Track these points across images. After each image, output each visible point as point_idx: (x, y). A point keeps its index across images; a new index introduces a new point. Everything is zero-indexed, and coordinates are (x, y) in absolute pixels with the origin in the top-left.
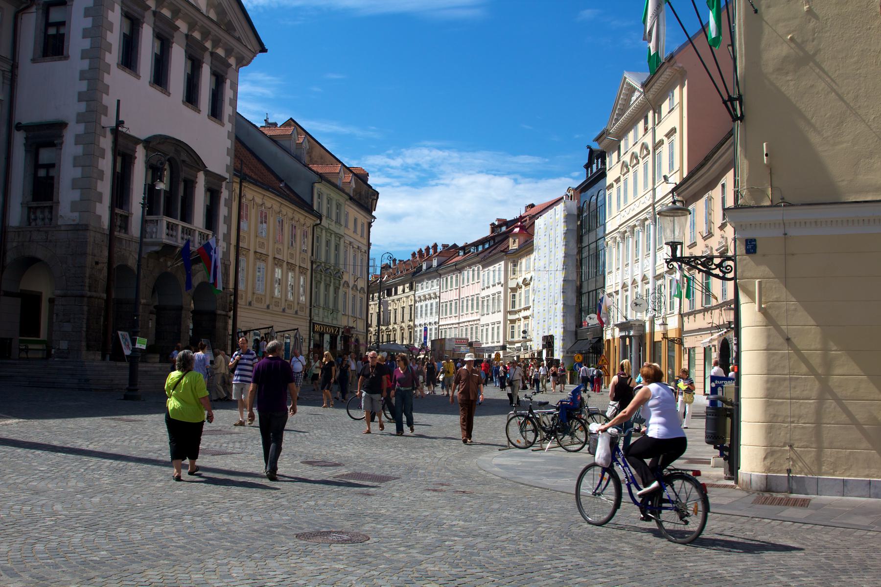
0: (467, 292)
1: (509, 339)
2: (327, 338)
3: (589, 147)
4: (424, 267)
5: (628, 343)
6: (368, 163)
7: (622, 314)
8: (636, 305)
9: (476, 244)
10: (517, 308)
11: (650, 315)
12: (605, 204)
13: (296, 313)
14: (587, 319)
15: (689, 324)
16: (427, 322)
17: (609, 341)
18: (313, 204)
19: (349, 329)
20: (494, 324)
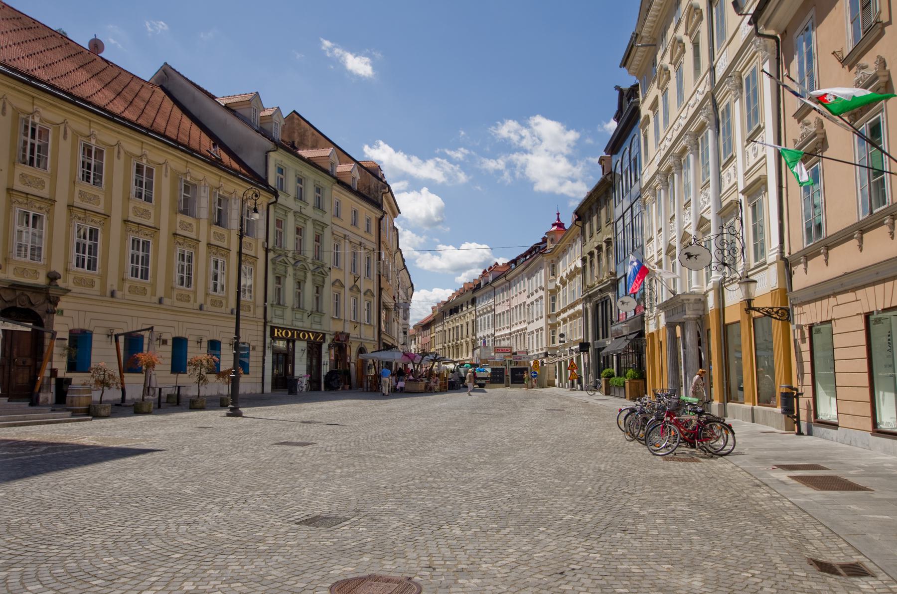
0: (516, 302)
1: (552, 345)
2: (301, 347)
3: (617, 88)
4: (482, 284)
5: (679, 334)
6: (382, 155)
7: (667, 286)
8: (689, 256)
9: (524, 255)
10: (557, 310)
11: (716, 276)
12: (639, 152)
13: (160, 301)
14: (619, 304)
15: (802, 278)
16: (485, 334)
17: (652, 334)
18: (267, 178)
19: (337, 335)
20: (537, 331)
